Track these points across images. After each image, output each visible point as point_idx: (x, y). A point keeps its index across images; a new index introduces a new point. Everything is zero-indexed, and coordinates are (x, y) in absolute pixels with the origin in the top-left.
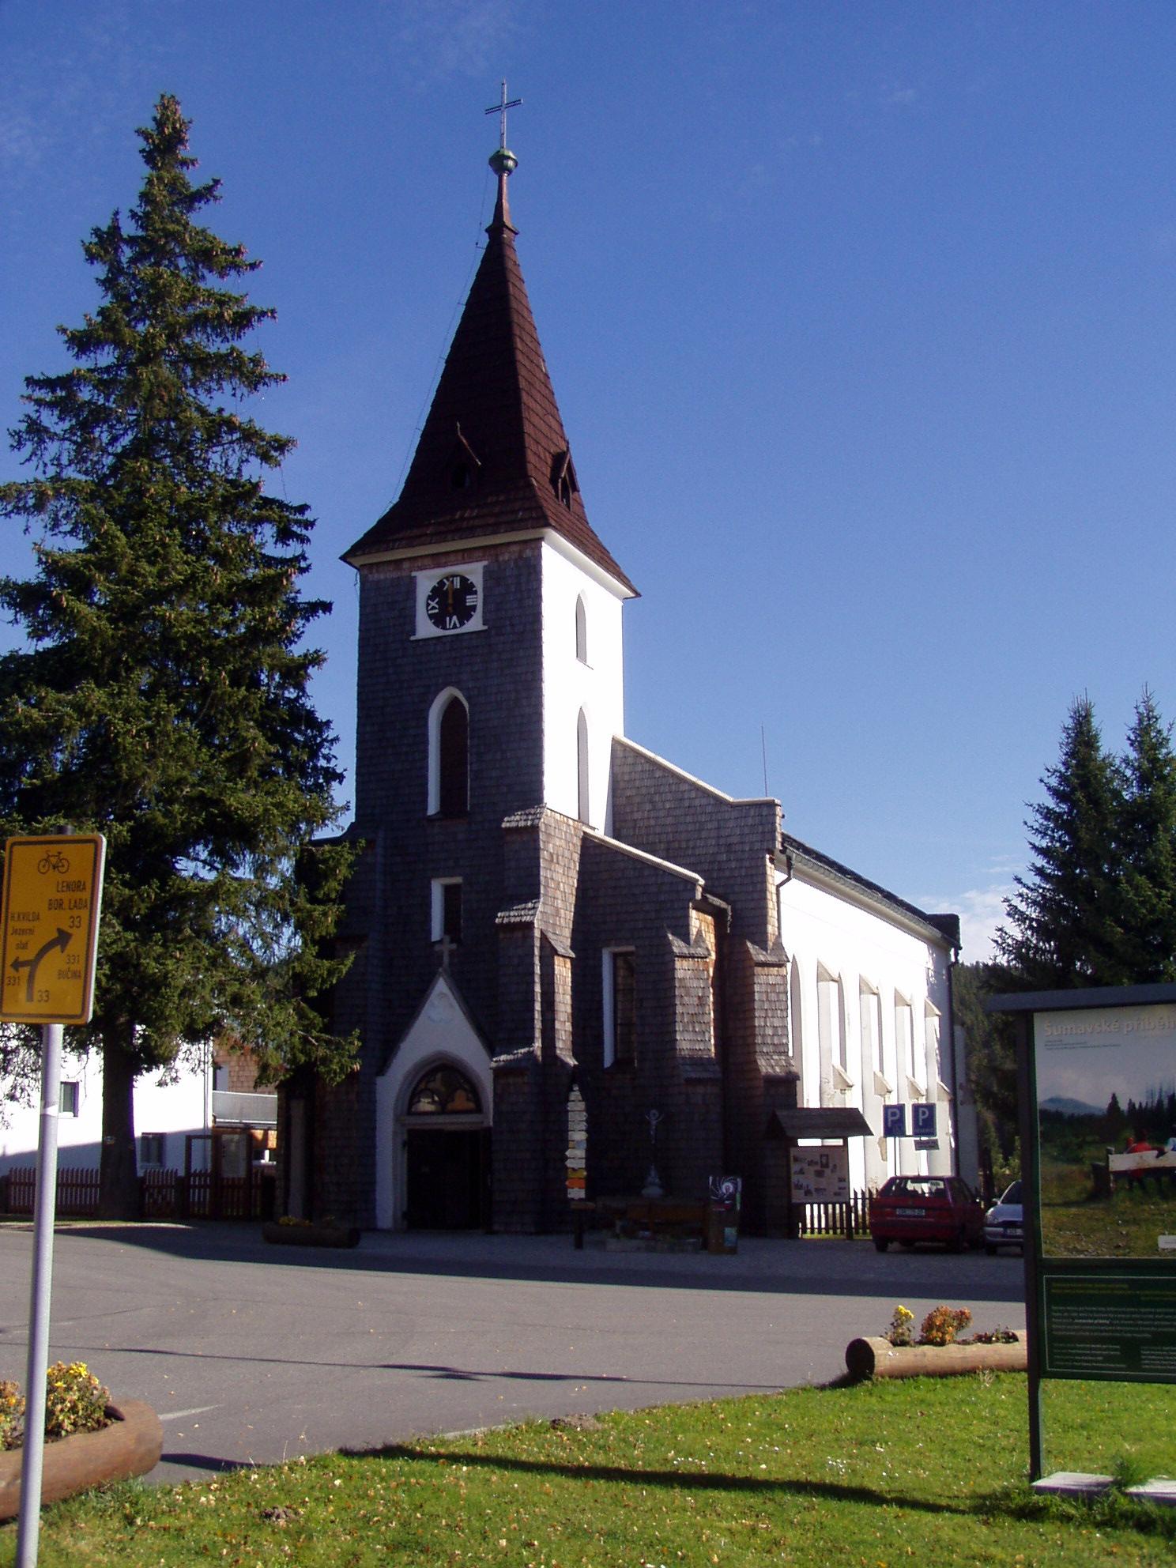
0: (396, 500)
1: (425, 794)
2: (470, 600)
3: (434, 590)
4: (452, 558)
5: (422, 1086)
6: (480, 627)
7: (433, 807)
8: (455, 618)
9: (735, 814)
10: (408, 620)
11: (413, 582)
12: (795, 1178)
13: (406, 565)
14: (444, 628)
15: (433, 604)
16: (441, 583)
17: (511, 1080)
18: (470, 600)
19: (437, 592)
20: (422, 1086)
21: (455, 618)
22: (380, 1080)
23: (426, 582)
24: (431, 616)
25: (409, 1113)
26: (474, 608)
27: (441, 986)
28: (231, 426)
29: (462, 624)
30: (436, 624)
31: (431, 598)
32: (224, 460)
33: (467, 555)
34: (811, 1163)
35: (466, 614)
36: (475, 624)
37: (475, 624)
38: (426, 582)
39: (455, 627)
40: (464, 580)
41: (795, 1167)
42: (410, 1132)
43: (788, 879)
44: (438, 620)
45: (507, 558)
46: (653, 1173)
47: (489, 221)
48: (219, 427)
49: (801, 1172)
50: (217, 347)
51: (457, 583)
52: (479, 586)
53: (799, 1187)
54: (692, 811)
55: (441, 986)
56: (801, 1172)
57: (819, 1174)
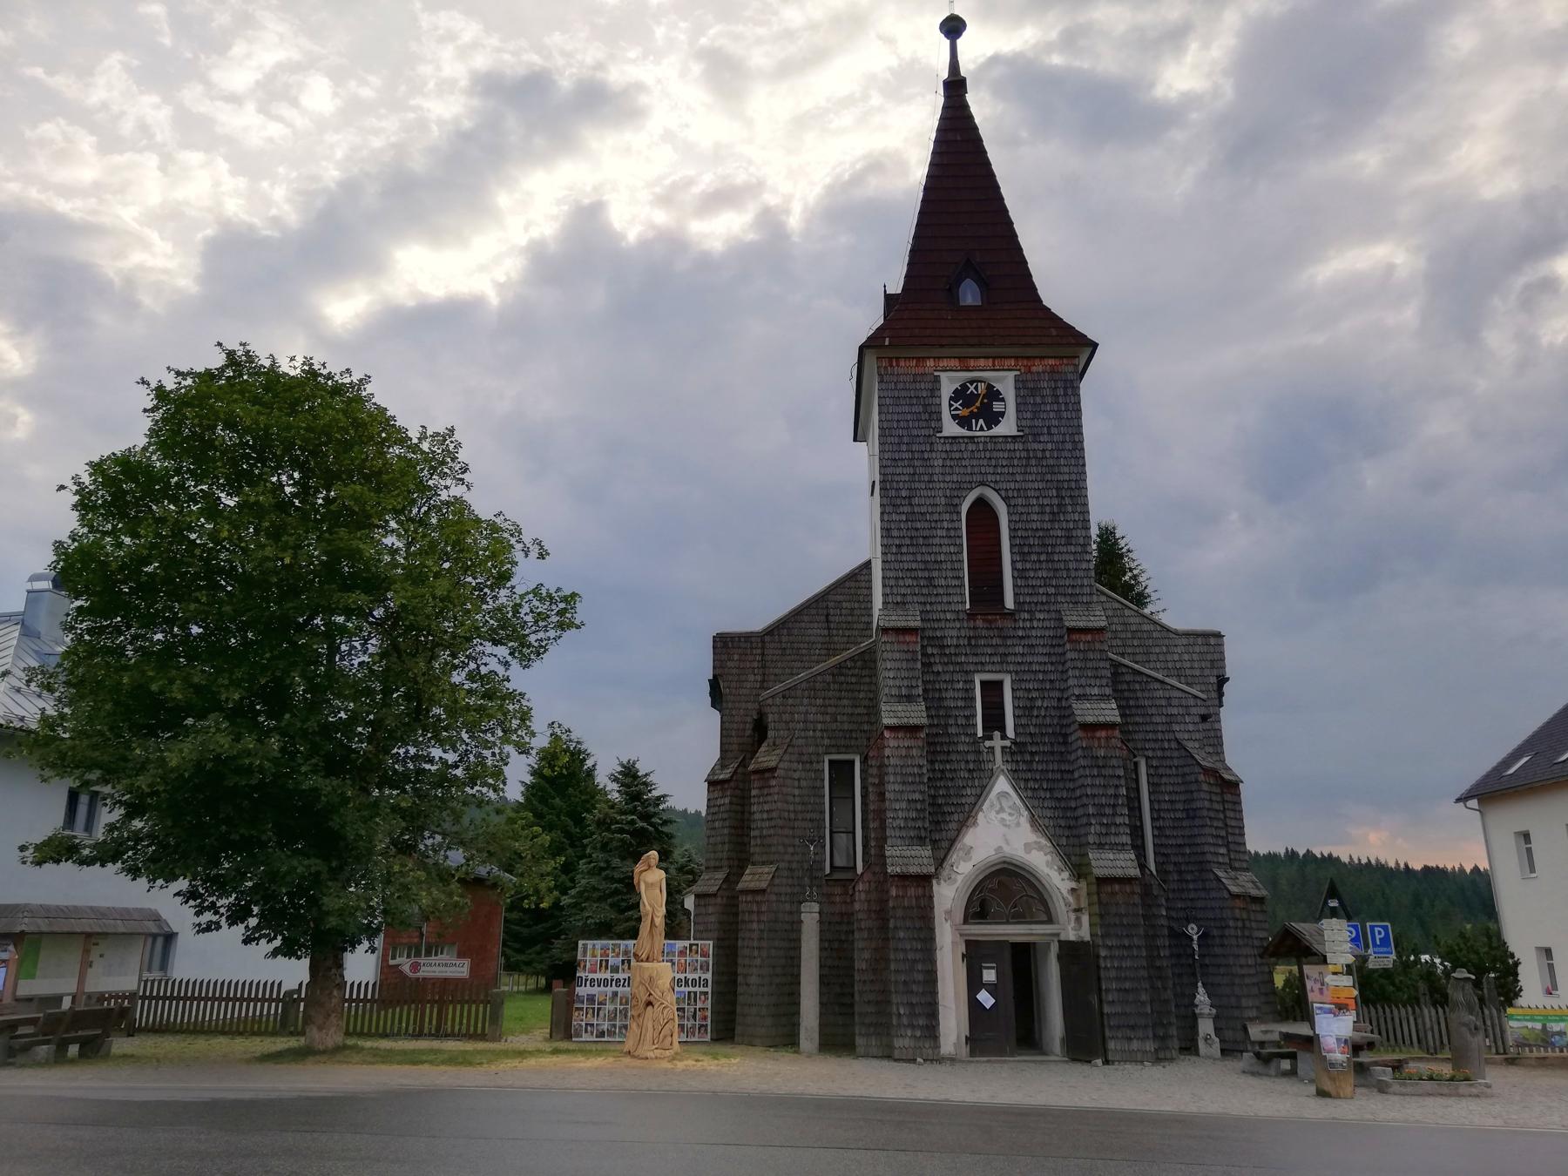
2: (997, 407)
4: (982, 362)
6: (1014, 432)
8: (981, 421)
9: (1185, 641)
11: (937, 380)
13: (930, 363)
14: (970, 429)
16: (964, 387)
19: (960, 394)
21: (981, 421)
23: (948, 384)
24: (954, 417)
26: (1002, 414)
27: (1002, 784)
29: (989, 428)
30: (961, 424)
33: (998, 362)
35: (994, 419)
36: (1007, 427)
38: (948, 384)
39: (982, 429)
40: (990, 387)
42: (968, 943)
44: (963, 422)
45: (1040, 369)
46: (1201, 990)
51: (982, 388)
55: (1002, 784)
57: (1321, 990)
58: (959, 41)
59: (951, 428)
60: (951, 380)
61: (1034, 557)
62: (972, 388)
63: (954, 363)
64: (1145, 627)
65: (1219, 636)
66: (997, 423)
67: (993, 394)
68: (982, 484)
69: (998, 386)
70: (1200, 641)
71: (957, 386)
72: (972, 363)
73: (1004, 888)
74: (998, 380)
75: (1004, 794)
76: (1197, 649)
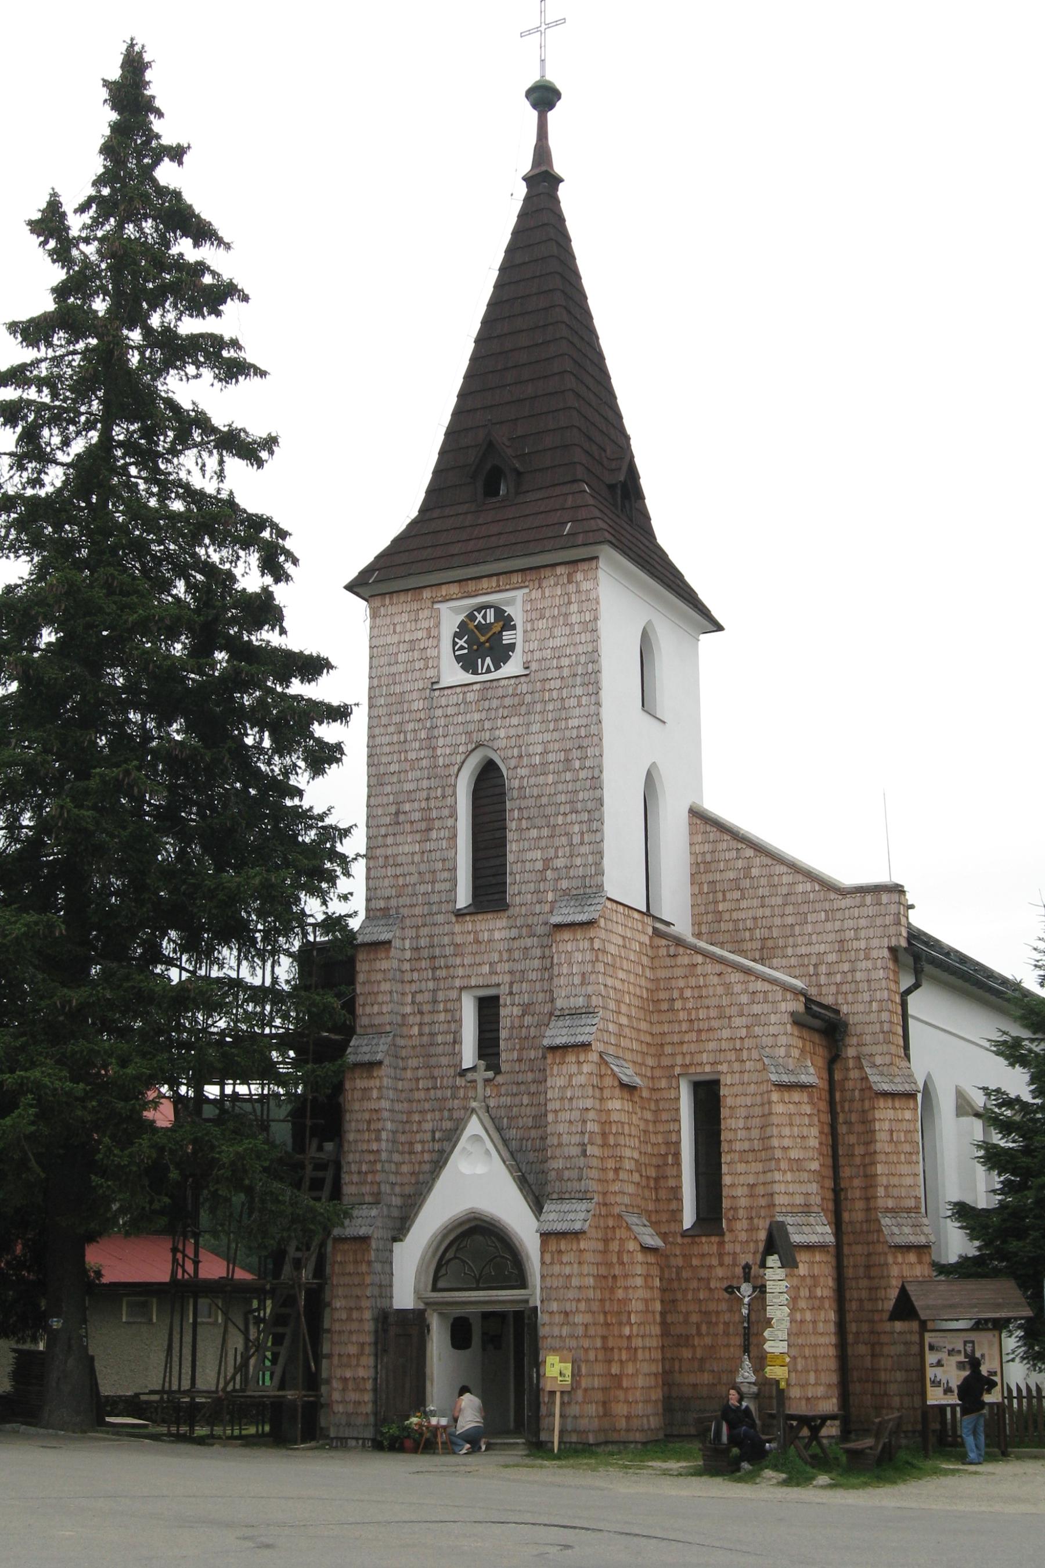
0: (414, 513)
1: (454, 881)
2: (507, 637)
3: (462, 625)
4: (485, 583)
5: (448, 1256)
7: (463, 898)
8: (488, 660)
10: (430, 662)
12: (930, 1373)
14: (475, 673)
15: (461, 643)
16: (471, 617)
17: (563, 1245)
18: (507, 637)
20: (448, 1256)
21: (488, 660)
22: (397, 1246)
24: (458, 658)
25: (435, 1289)
26: (512, 647)
27: (474, 1127)
28: (202, 421)
29: (497, 667)
30: (465, 668)
31: (457, 635)
32: (195, 469)
34: (951, 1352)
35: (502, 654)
37: (512, 667)
38: (450, 617)
39: (488, 671)
40: (499, 613)
41: (931, 1358)
43: (916, 986)
44: (468, 663)
47: (525, 165)
48: (191, 425)
49: (939, 1364)
50: (189, 326)
52: (518, 619)
53: (936, 1383)
54: (793, 899)
56: (939, 1364)
58: (553, 116)
59: (453, 674)
60: (454, 610)
61: (534, 833)
62: (479, 617)
63: (454, 589)
64: (800, 888)
65: (898, 890)
66: (506, 659)
67: (506, 623)
68: (479, 745)
69: (509, 610)
70: (869, 899)
71: (462, 617)
72: (471, 586)
73: (479, 1247)
74: (511, 602)
75: (476, 1138)
76: (865, 911)
